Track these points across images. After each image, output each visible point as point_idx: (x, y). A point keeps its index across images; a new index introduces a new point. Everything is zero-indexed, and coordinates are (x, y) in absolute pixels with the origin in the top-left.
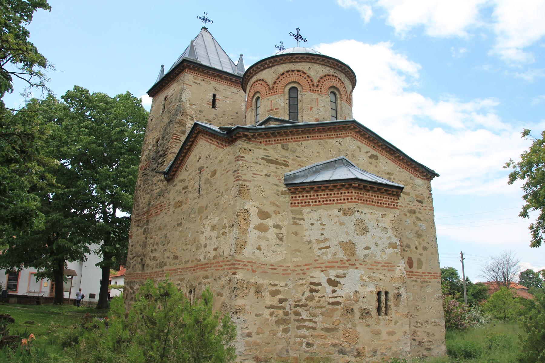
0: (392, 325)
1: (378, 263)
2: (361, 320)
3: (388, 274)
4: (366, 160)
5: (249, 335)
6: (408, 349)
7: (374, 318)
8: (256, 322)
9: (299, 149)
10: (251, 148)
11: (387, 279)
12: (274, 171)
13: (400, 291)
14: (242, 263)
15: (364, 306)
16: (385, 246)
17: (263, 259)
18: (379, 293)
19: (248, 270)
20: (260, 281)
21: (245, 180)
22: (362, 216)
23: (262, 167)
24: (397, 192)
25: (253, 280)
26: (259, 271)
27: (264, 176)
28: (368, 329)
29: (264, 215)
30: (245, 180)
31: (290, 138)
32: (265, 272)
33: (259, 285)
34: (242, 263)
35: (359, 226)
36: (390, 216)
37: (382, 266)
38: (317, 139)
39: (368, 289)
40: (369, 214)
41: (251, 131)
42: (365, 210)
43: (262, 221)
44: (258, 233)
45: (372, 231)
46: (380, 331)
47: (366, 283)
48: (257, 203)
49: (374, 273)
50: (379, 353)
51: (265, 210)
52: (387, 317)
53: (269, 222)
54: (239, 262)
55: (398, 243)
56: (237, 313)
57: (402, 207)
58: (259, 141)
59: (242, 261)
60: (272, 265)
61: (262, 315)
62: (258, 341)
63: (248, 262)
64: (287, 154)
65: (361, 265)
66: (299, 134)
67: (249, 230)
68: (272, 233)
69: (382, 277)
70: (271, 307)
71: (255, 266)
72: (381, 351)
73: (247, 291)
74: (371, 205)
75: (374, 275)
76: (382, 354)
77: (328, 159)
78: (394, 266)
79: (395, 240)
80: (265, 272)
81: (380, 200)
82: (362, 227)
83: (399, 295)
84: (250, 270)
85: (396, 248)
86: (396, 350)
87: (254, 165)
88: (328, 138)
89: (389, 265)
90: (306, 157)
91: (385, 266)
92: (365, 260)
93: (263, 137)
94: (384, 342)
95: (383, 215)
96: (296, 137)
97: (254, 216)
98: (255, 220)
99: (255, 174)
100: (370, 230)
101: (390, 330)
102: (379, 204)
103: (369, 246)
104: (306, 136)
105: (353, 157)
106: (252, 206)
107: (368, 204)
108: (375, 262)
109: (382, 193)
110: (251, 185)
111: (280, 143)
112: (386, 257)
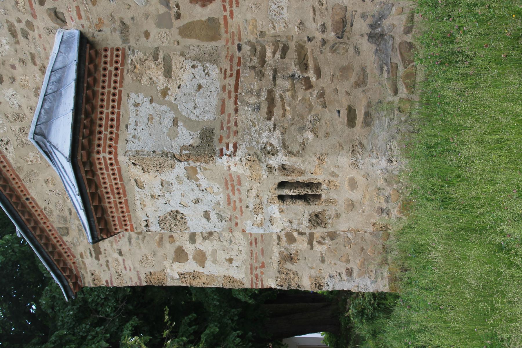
0: (337, 181)
1: (229, 199)
2: (329, 226)
3: (246, 184)
4: (11, 91)
5: (349, 272)
6: (384, 163)
7: (325, 208)
8: (333, 262)
9: (56, 213)
10: (89, 274)
11: (255, 186)
12: (109, 245)
13: (277, 166)
14: (255, 281)
15: (306, 223)
16: (195, 187)
17: (244, 255)
18: (281, 198)
19: (262, 273)
20: (276, 256)
21: (139, 278)
22: (153, 221)
23: (110, 260)
24: (84, 164)
25: (276, 266)
26: (261, 259)
27: (123, 257)
28: (343, 215)
29: (180, 255)
30: (139, 278)
31: (45, 226)
32: (262, 250)
33: (282, 258)
34: (255, 281)
35: (173, 226)
36: (136, 172)
37: (234, 194)
38: (22, 184)
39: (277, 215)
40: (145, 209)
41: (66, 283)
42: (141, 215)
43: (190, 257)
44: (208, 263)
45: (174, 206)
46: (347, 200)
47: (267, 218)
48: (167, 263)
49: (247, 207)
50: (384, 206)
51: (173, 254)
52: (324, 186)
53: (189, 248)
54: (254, 284)
55: (184, 164)
56: (320, 285)
57: (78, 8)
58: (72, 265)
59: (252, 280)
60: (251, 244)
61: (322, 254)
62: (358, 261)
63: (252, 273)
64: (74, 227)
65: (237, 224)
66: (30, 215)
67: (208, 274)
68: (207, 247)
69: (253, 193)
70: (310, 243)
71: (256, 265)
72: (382, 201)
73: (291, 274)
74: (127, 205)
75: (251, 206)
76: (387, 201)
77: (49, 166)
78: (230, 175)
79: (180, 168)
80: (262, 250)
81: (112, 191)
82: (173, 222)
83: (283, 168)
84: (263, 270)
85: (194, 170)
86: (382, 181)
87: (112, 269)
88: (10, 166)
89: (229, 183)
90: (64, 201)
91: (233, 189)
92: (228, 219)
93: (65, 263)
94: (367, 197)
95: (139, 185)
96: (39, 218)
97: (186, 267)
98: (190, 266)
99: (125, 268)
100: (175, 209)
101: (346, 183)
102: (121, 192)
103: (202, 213)
104: (27, 202)
105: (18, 118)
106: (172, 270)
107: (128, 211)
108: (229, 204)
109: (97, 187)
110: (143, 271)
111: (61, 238)
112: (216, 187)
